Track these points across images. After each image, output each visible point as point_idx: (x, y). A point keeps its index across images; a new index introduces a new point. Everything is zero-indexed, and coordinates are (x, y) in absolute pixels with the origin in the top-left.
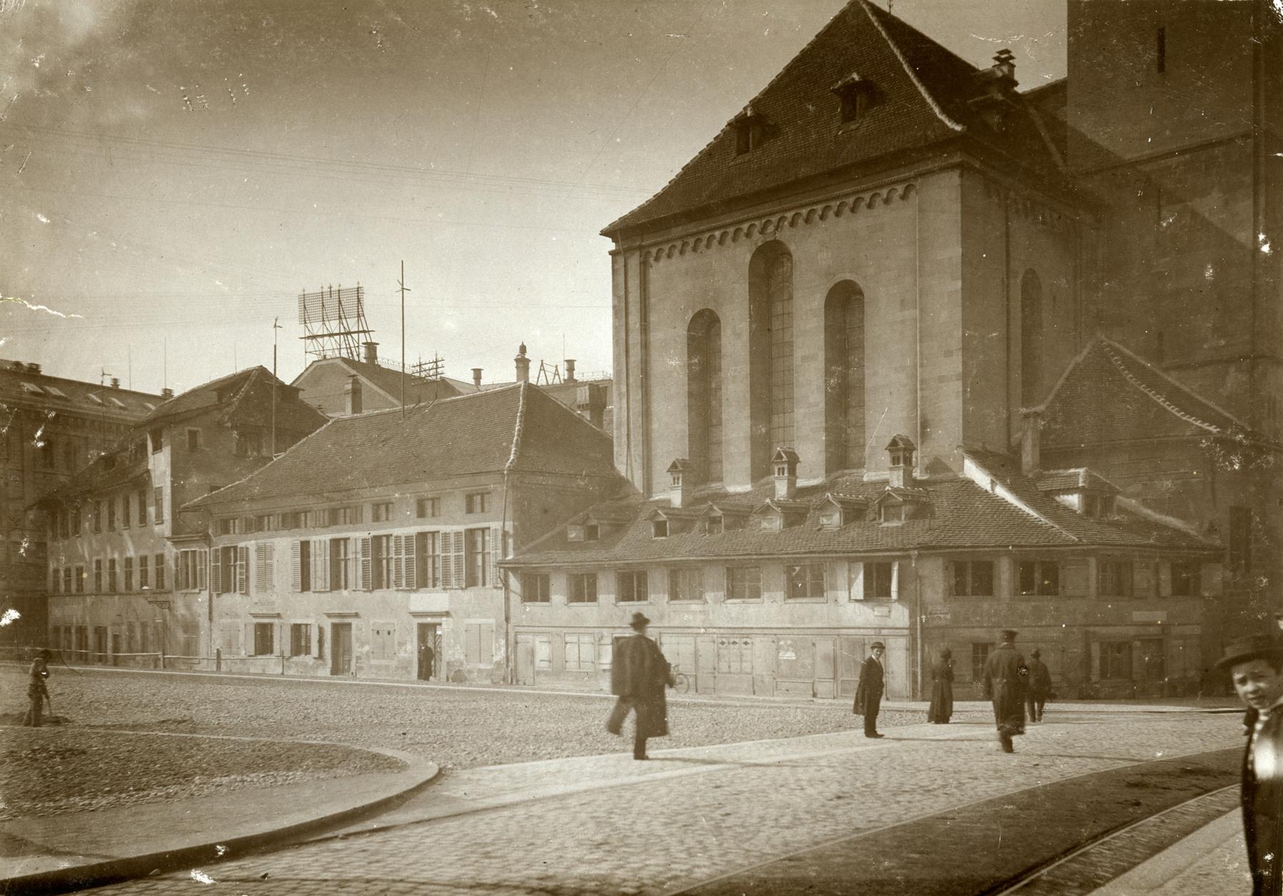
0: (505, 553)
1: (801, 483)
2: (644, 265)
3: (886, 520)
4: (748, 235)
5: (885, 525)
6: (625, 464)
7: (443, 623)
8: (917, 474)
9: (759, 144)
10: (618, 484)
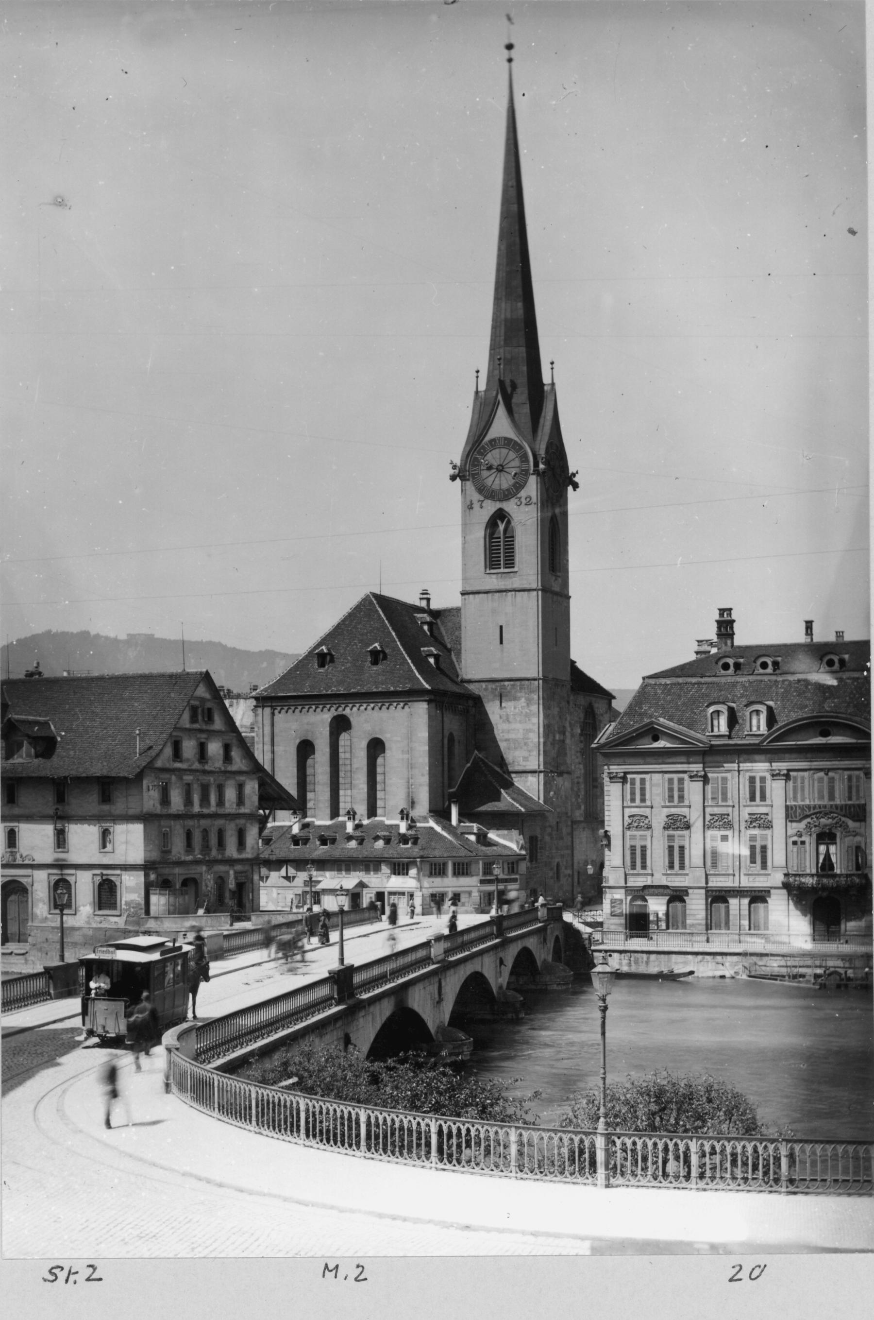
2: (273, 714)
4: (329, 710)
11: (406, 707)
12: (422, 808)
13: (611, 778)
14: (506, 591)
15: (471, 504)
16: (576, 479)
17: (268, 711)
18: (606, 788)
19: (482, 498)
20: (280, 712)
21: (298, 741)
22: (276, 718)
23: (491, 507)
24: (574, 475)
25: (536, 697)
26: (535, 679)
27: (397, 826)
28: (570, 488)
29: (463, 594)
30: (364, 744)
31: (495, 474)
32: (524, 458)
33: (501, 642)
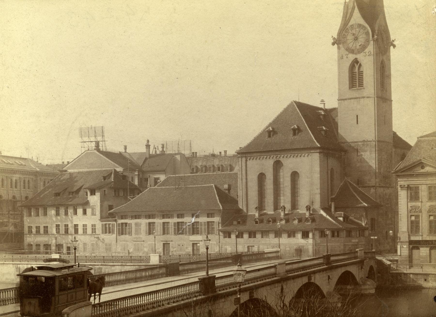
0: (219, 227)
1: (286, 212)
2: (246, 161)
3: (307, 223)
5: (307, 224)
6: (241, 205)
7: (200, 243)
8: (311, 212)
9: (273, 135)
10: (239, 211)
11: (309, 156)
12: (317, 205)
13: (401, 188)
14: (359, 98)
15: (342, 56)
16: (395, 43)
17: (244, 159)
18: (399, 193)
19: (347, 53)
20: (250, 160)
21: (258, 173)
22: (248, 163)
23: (352, 57)
24: (393, 41)
25: (374, 150)
27: (305, 214)
28: (392, 47)
29: (338, 100)
30: (289, 174)
31: (353, 41)
32: (367, 33)
33: (357, 123)
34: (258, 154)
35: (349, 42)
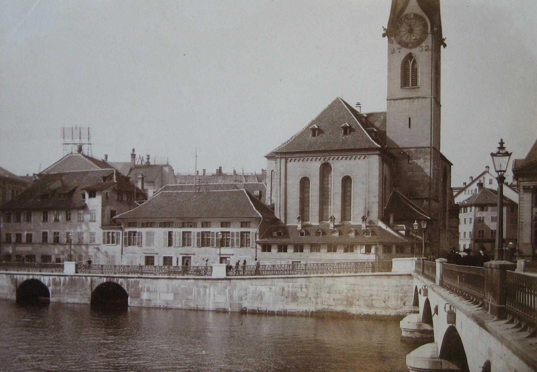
0: (256, 239)
1: (335, 224)
2: (286, 162)
3: (366, 235)
4: (320, 160)
5: (366, 236)
6: (278, 214)
7: (231, 258)
9: (318, 134)
10: (276, 221)
11: (366, 158)
14: (413, 98)
15: (394, 50)
16: (445, 42)
17: (283, 161)
19: (400, 47)
20: (290, 161)
21: (301, 178)
23: (405, 52)
24: (444, 40)
25: (429, 157)
26: (429, 147)
28: (442, 46)
29: (387, 100)
30: (340, 179)
32: (425, 25)
33: (410, 127)
34: (302, 155)
35: (402, 33)
